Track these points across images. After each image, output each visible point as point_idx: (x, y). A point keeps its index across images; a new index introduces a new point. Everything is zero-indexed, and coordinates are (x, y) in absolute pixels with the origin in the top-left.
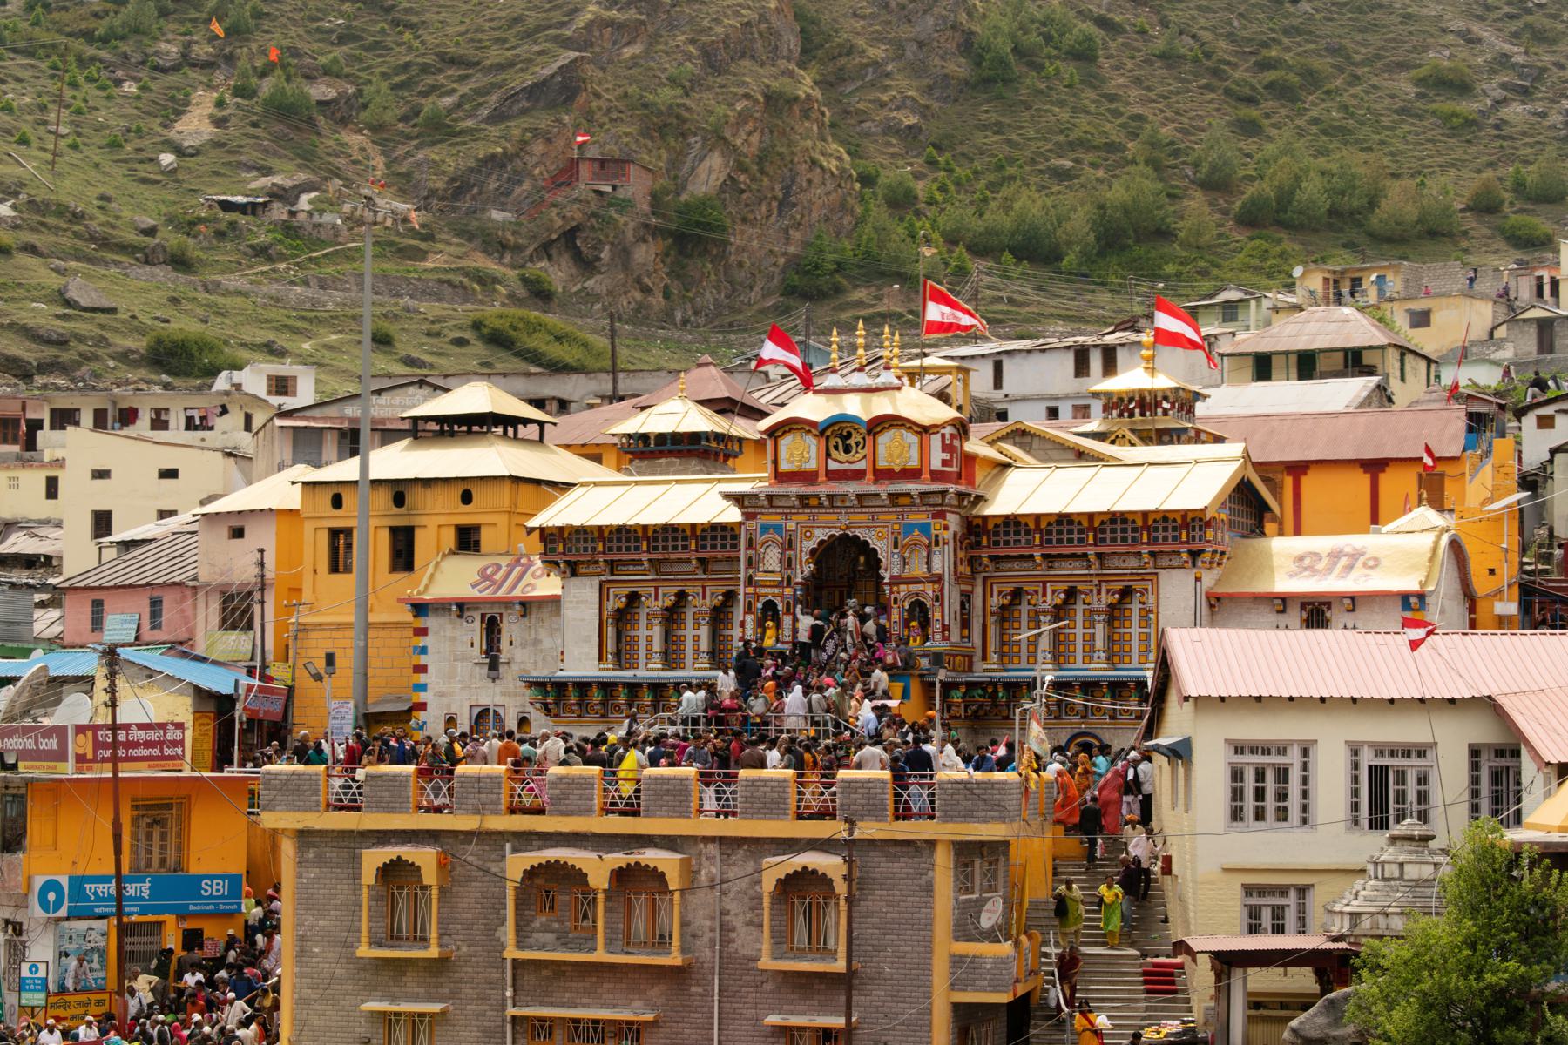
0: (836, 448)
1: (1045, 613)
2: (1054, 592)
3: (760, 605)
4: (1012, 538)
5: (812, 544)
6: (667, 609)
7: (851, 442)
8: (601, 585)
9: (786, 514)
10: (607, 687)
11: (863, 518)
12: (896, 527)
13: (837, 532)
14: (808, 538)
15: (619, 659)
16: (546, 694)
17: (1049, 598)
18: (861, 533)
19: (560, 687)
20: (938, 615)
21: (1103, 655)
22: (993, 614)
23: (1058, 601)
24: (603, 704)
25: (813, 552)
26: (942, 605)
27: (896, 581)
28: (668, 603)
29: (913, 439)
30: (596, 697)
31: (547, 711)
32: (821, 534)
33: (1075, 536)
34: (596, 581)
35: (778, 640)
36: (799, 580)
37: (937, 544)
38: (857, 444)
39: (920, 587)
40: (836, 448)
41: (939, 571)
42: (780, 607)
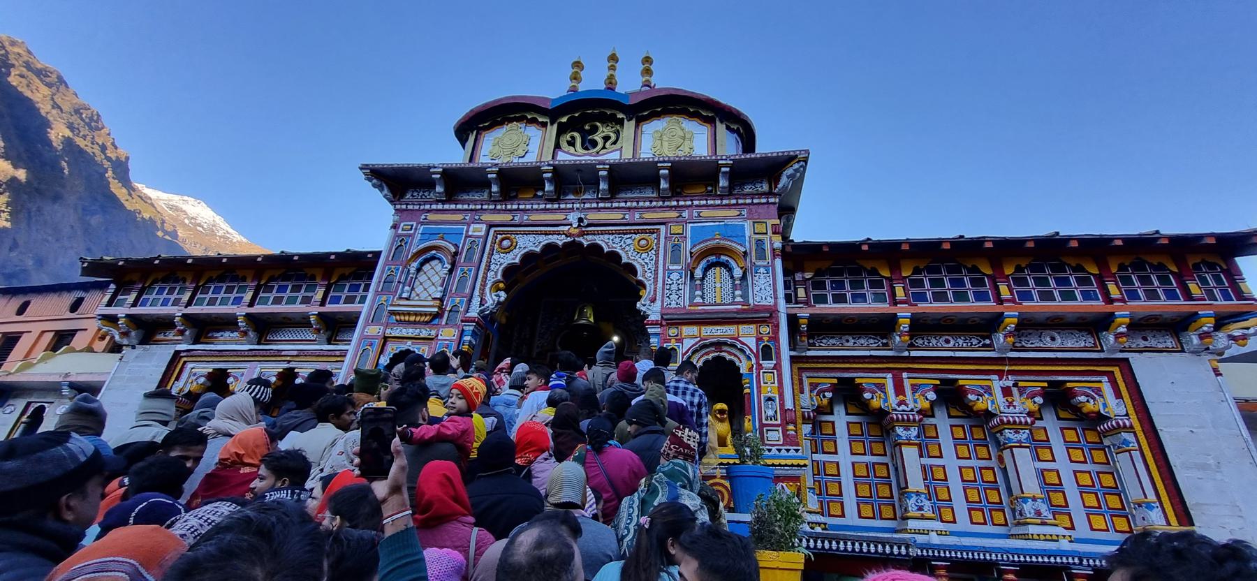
2: (915, 388)
4: (848, 291)
5: (514, 257)
7: (598, 137)
11: (616, 216)
12: (676, 229)
13: (560, 241)
14: (507, 250)
18: (607, 243)
20: (770, 389)
21: (1044, 508)
22: (805, 420)
23: (927, 405)
25: (509, 271)
26: (778, 367)
27: (672, 320)
32: (529, 243)
36: (474, 313)
37: (761, 255)
38: (606, 139)
39: (730, 330)
40: (572, 143)
41: (771, 302)
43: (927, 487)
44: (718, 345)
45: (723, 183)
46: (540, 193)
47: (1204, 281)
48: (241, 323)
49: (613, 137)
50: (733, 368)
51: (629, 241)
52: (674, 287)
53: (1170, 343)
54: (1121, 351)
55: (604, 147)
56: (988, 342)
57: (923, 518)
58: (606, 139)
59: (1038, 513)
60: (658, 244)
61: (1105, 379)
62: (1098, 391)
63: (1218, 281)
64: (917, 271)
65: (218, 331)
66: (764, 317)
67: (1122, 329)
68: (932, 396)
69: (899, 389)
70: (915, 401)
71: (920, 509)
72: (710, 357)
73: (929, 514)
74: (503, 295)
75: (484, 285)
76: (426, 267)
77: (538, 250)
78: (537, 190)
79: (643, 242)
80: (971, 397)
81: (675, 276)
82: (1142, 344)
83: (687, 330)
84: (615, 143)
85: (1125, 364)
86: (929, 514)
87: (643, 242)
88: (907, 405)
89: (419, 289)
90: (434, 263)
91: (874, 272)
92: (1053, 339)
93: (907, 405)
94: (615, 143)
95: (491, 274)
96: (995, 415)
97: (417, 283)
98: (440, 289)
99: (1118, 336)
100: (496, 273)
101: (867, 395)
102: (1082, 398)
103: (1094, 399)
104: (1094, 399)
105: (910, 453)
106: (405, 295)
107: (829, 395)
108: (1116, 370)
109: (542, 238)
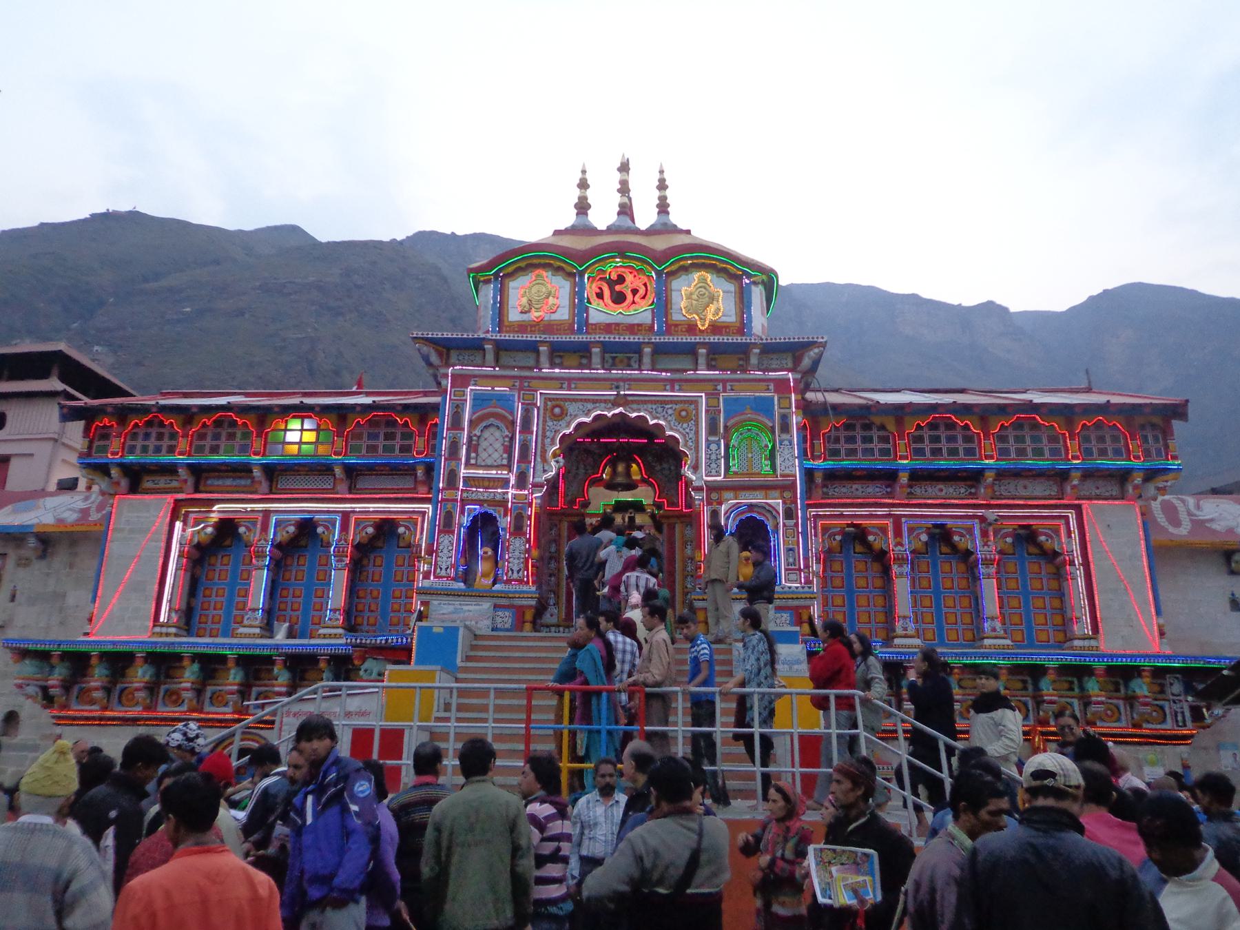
0: (600, 296)
1: (900, 560)
2: (911, 530)
3: (466, 520)
4: (859, 445)
6: (278, 546)
8: (177, 502)
9: (521, 378)
10: (164, 663)
15: (188, 623)
16: (52, 667)
17: (906, 541)
19: (78, 662)
21: (998, 625)
23: (919, 545)
24: (152, 688)
28: (283, 536)
29: (722, 289)
30: (141, 674)
31: (48, 699)
33: (961, 445)
34: (169, 500)
35: (494, 583)
37: (785, 428)
38: (635, 292)
40: (600, 296)
42: (505, 522)
43: (915, 613)
44: (751, 507)
45: (754, 360)
46: (584, 361)
47: (1145, 438)
48: (257, 473)
49: (642, 291)
50: (762, 525)
51: (670, 412)
52: (713, 457)
53: (1115, 491)
54: (1078, 499)
55: (634, 302)
56: (973, 490)
57: (906, 636)
58: (635, 292)
59: (994, 630)
60: (697, 415)
61: (1063, 521)
62: (1057, 532)
63: (1156, 439)
64: (919, 427)
65: (219, 478)
66: (786, 487)
67: (1075, 482)
68: (924, 537)
69: (898, 533)
70: (910, 543)
71: (905, 629)
72: (743, 517)
73: (911, 632)
74: (560, 459)
75: (544, 452)
76: (487, 434)
77: (587, 420)
78: (582, 357)
79: (684, 413)
80: (956, 538)
81: (713, 447)
82: (1095, 492)
83: (727, 495)
84: (644, 297)
85: (1078, 509)
86: (911, 632)
87: (684, 413)
88: (902, 545)
89: (484, 455)
90: (492, 430)
91: (882, 427)
92: (1025, 487)
93: (902, 545)
94: (644, 297)
95: (548, 441)
96: (972, 553)
97: (480, 450)
98: (505, 456)
99: (1074, 487)
100: (553, 440)
101: (871, 538)
102: (1043, 538)
103: (1051, 538)
104: (1051, 538)
105: (902, 587)
106: (473, 461)
107: (838, 538)
108: (1072, 515)
109: (590, 406)
